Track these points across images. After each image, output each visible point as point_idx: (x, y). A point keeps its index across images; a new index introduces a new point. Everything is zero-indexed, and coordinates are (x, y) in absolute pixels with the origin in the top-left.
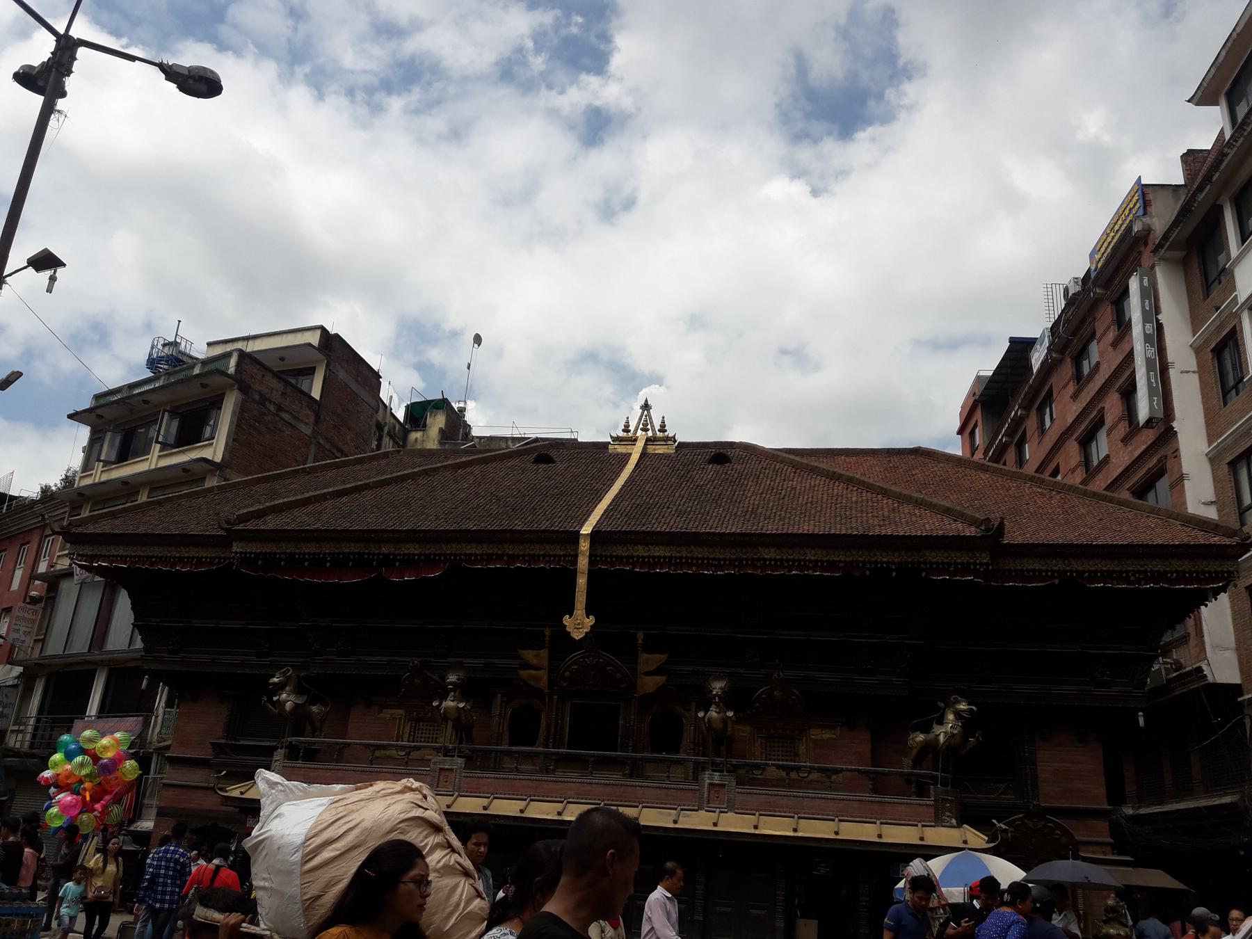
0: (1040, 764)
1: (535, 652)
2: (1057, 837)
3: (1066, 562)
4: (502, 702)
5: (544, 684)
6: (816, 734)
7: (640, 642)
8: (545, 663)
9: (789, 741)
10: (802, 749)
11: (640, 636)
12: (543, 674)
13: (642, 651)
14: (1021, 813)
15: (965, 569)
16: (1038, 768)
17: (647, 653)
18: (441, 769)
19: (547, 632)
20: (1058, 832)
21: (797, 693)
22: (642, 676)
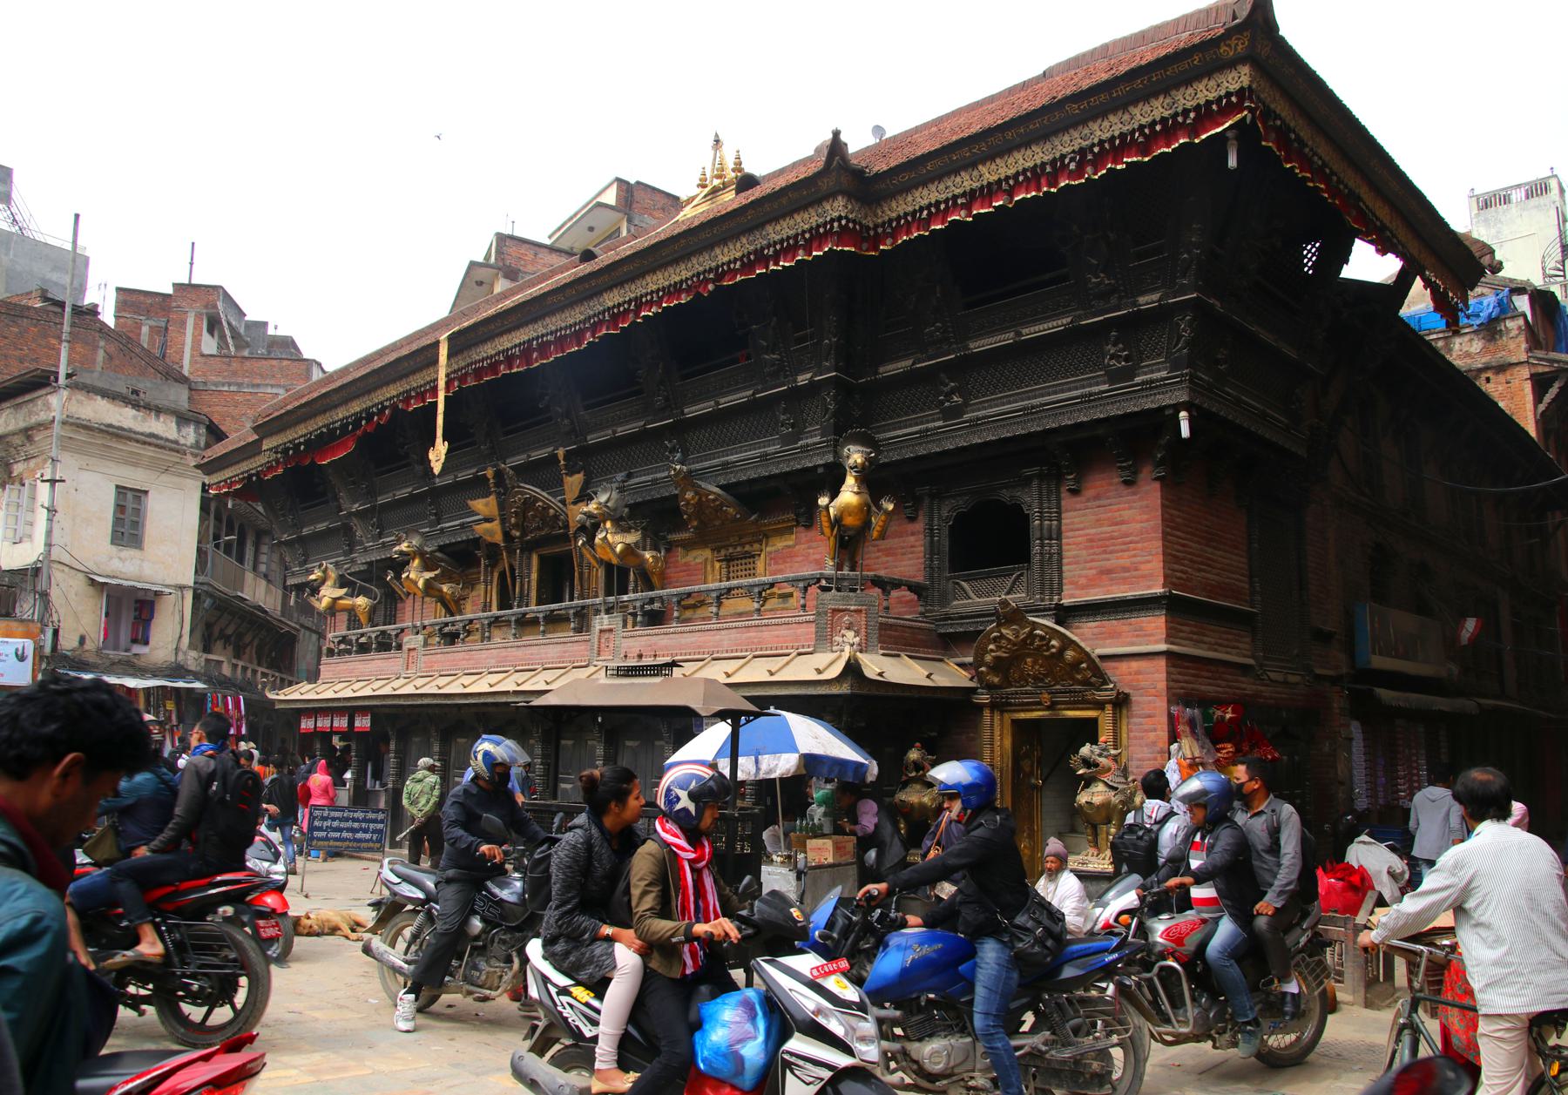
0: (1070, 534)
1: (484, 501)
2: (1054, 650)
3: (975, 173)
4: (486, 566)
5: (498, 538)
6: (779, 544)
7: (562, 462)
8: (496, 512)
9: (751, 560)
10: (760, 564)
11: (561, 452)
12: (495, 526)
13: (566, 474)
14: (993, 622)
15: (816, 236)
16: (1064, 541)
17: (571, 474)
18: (410, 650)
19: (490, 473)
20: (1054, 642)
21: (717, 490)
22: (572, 506)
